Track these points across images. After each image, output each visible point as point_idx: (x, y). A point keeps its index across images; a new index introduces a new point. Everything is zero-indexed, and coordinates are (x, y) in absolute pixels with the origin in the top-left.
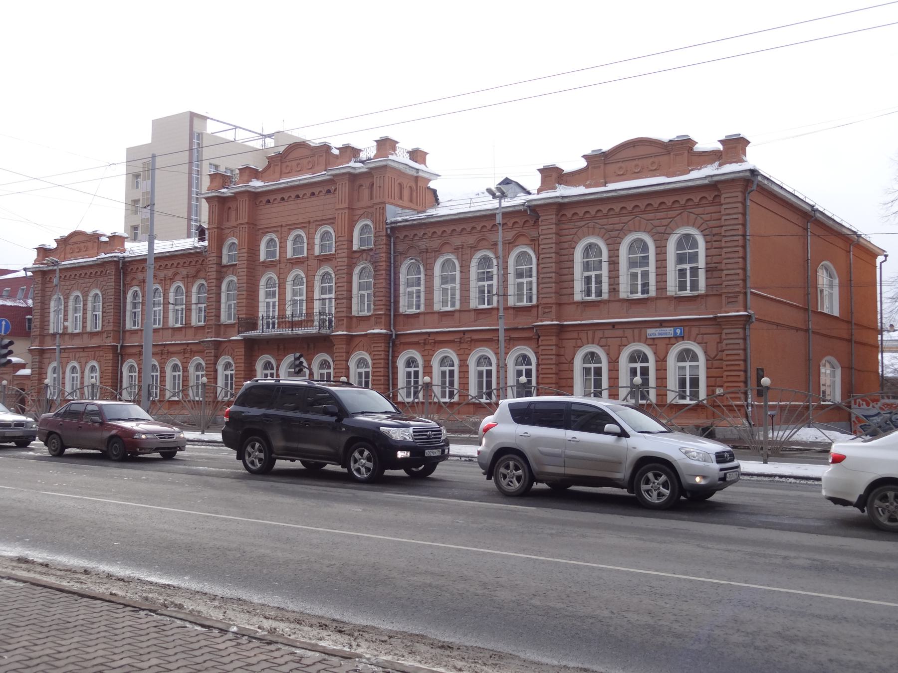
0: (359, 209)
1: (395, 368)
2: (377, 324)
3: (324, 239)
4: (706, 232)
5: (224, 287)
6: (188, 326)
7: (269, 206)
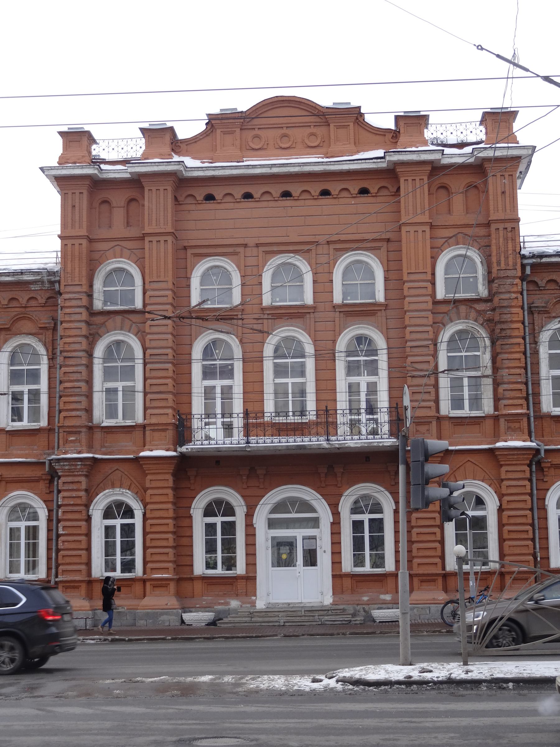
0: (446, 227)
1: (543, 509)
2: (514, 432)
3: (361, 276)
5: (99, 351)
7: (210, 205)
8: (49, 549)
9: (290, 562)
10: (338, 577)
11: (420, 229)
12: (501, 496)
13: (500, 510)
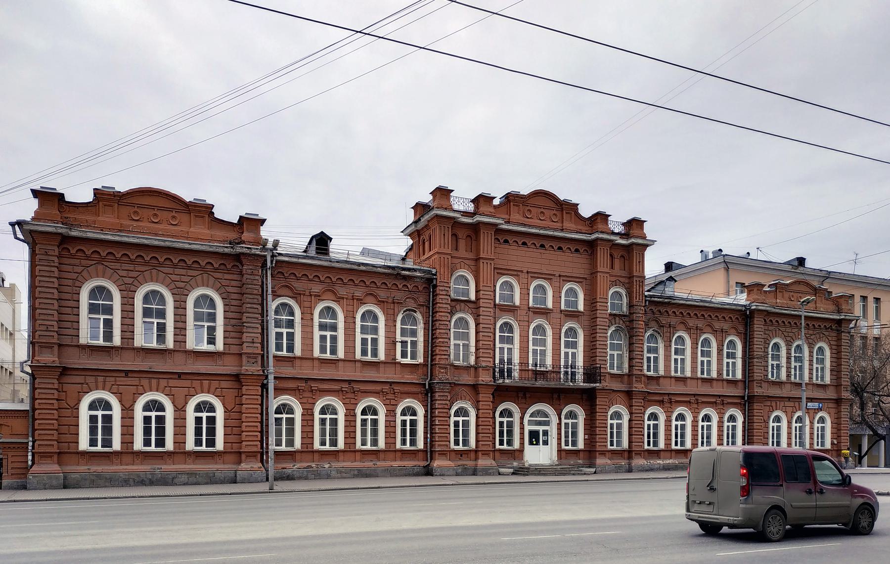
4: (123, 287)
6: (391, 362)
8: (425, 433)
9: (537, 444)
10: (560, 451)
11: (606, 275)
12: (631, 413)
13: (630, 420)
